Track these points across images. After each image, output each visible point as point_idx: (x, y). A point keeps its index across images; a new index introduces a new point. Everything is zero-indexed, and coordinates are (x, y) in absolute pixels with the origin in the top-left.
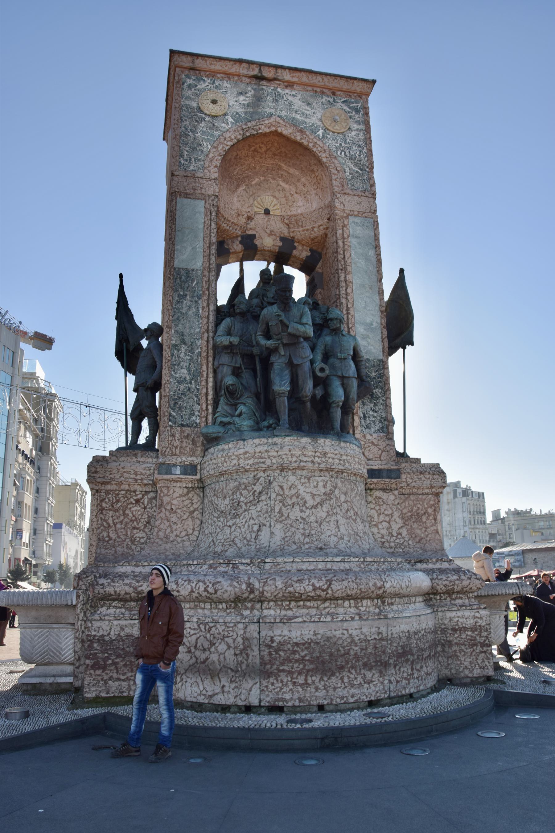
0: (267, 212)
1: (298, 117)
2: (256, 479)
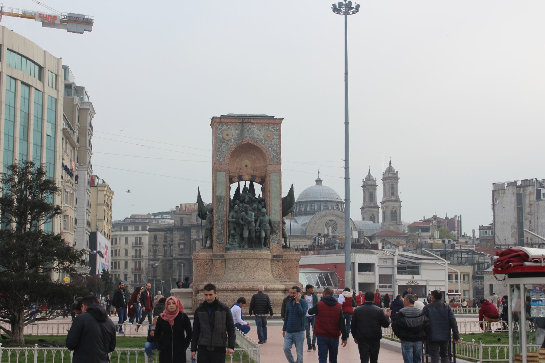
0: (246, 166)
1: (256, 136)
2: (238, 261)
